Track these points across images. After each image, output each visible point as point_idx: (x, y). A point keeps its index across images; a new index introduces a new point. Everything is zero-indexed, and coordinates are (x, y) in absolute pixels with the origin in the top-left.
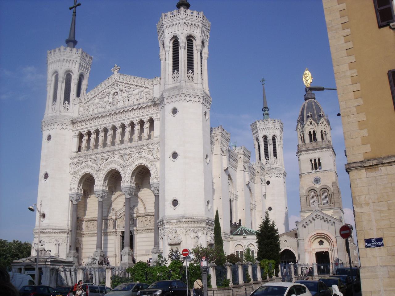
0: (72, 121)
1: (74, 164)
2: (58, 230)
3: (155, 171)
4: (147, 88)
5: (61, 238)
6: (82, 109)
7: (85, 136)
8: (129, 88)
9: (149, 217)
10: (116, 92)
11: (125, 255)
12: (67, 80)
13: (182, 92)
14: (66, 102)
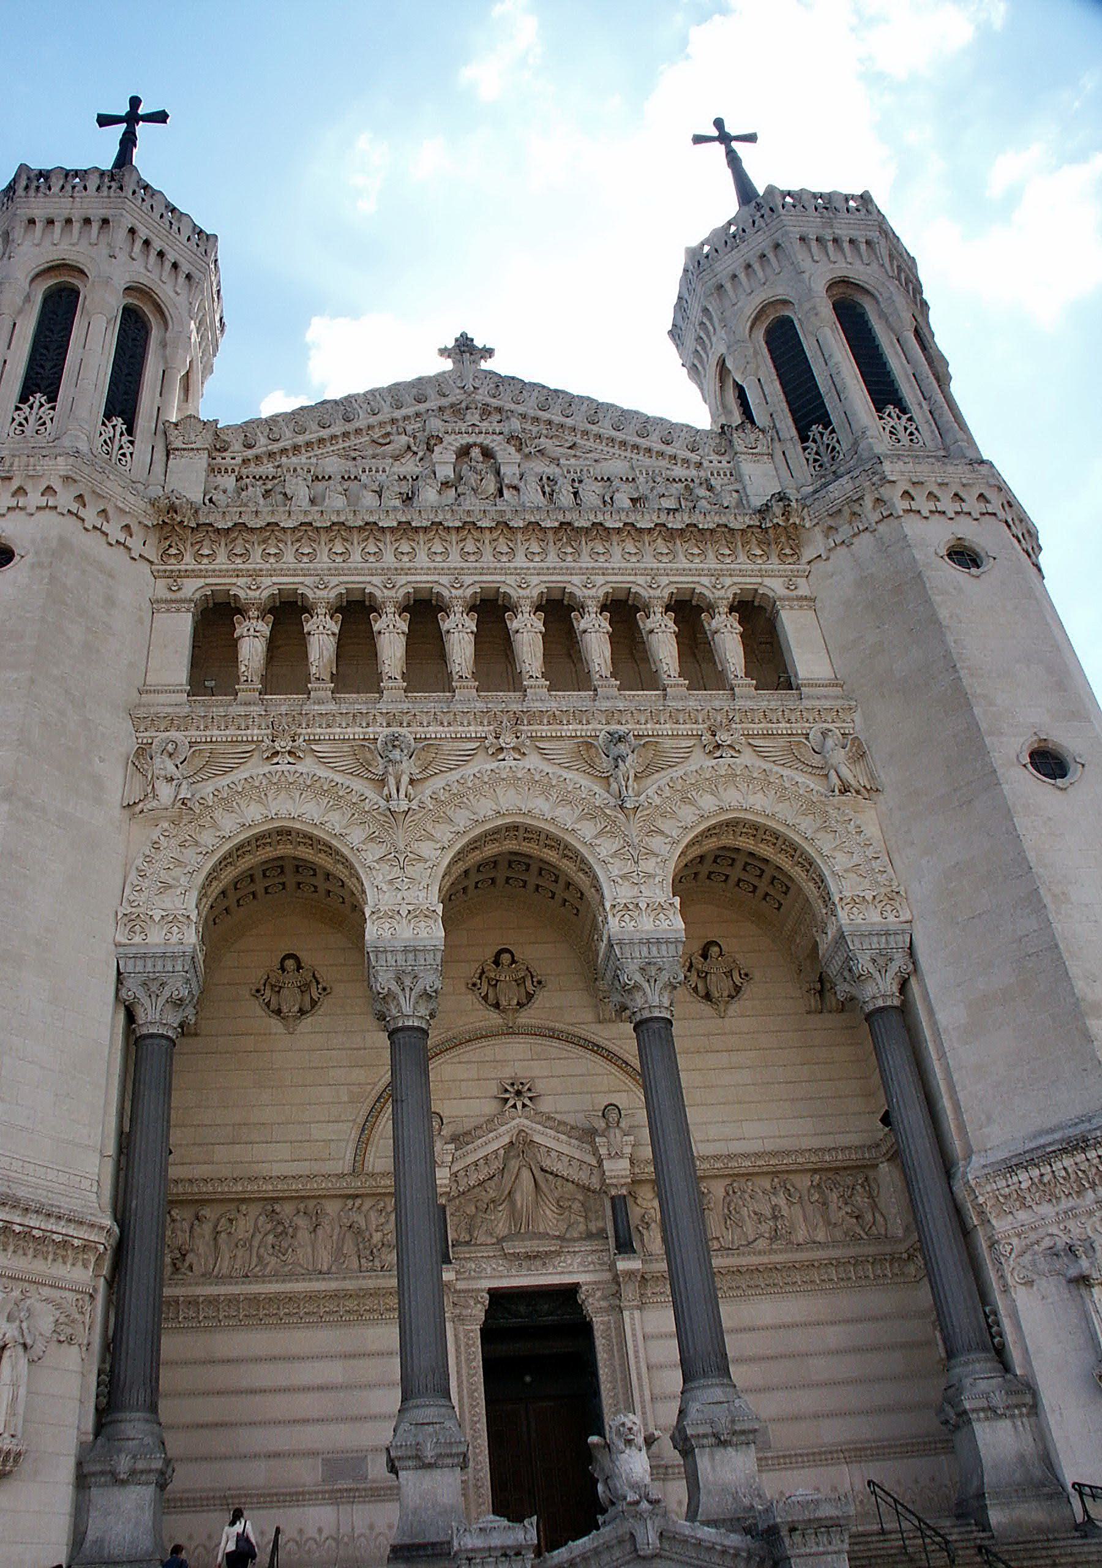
0: (173, 509)
1: (170, 755)
2: (33, 1221)
6: (229, 482)
7: (254, 613)
10: (475, 444)
12: (125, 331)
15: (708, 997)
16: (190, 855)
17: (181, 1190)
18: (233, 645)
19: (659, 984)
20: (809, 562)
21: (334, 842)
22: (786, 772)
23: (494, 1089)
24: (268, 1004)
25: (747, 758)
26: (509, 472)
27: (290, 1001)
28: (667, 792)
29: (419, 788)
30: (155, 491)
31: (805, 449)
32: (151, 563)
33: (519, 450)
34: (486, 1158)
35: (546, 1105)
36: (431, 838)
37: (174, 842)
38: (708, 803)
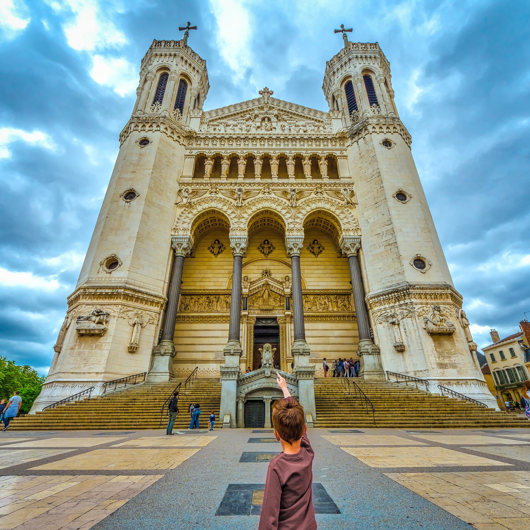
1: (187, 192)
3: (349, 220)
4: (319, 121)
5: (147, 312)
7: (209, 159)
8: (290, 117)
9: (312, 297)
10: (266, 117)
11: (302, 355)
13: (398, 123)
14: (178, 110)
15: (313, 253)
16: (190, 215)
17: (188, 292)
18: (204, 166)
19: (297, 248)
20: (347, 147)
21: (224, 213)
22: (334, 199)
23: (261, 271)
24: (211, 251)
25: (325, 195)
26: (274, 125)
27: (216, 250)
28: (304, 203)
29: (245, 201)
30: (187, 129)
31: (350, 117)
32: (185, 146)
33: (277, 119)
34: (258, 287)
35: (273, 276)
36: (246, 213)
37: (187, 212)
38: (314, 206)
